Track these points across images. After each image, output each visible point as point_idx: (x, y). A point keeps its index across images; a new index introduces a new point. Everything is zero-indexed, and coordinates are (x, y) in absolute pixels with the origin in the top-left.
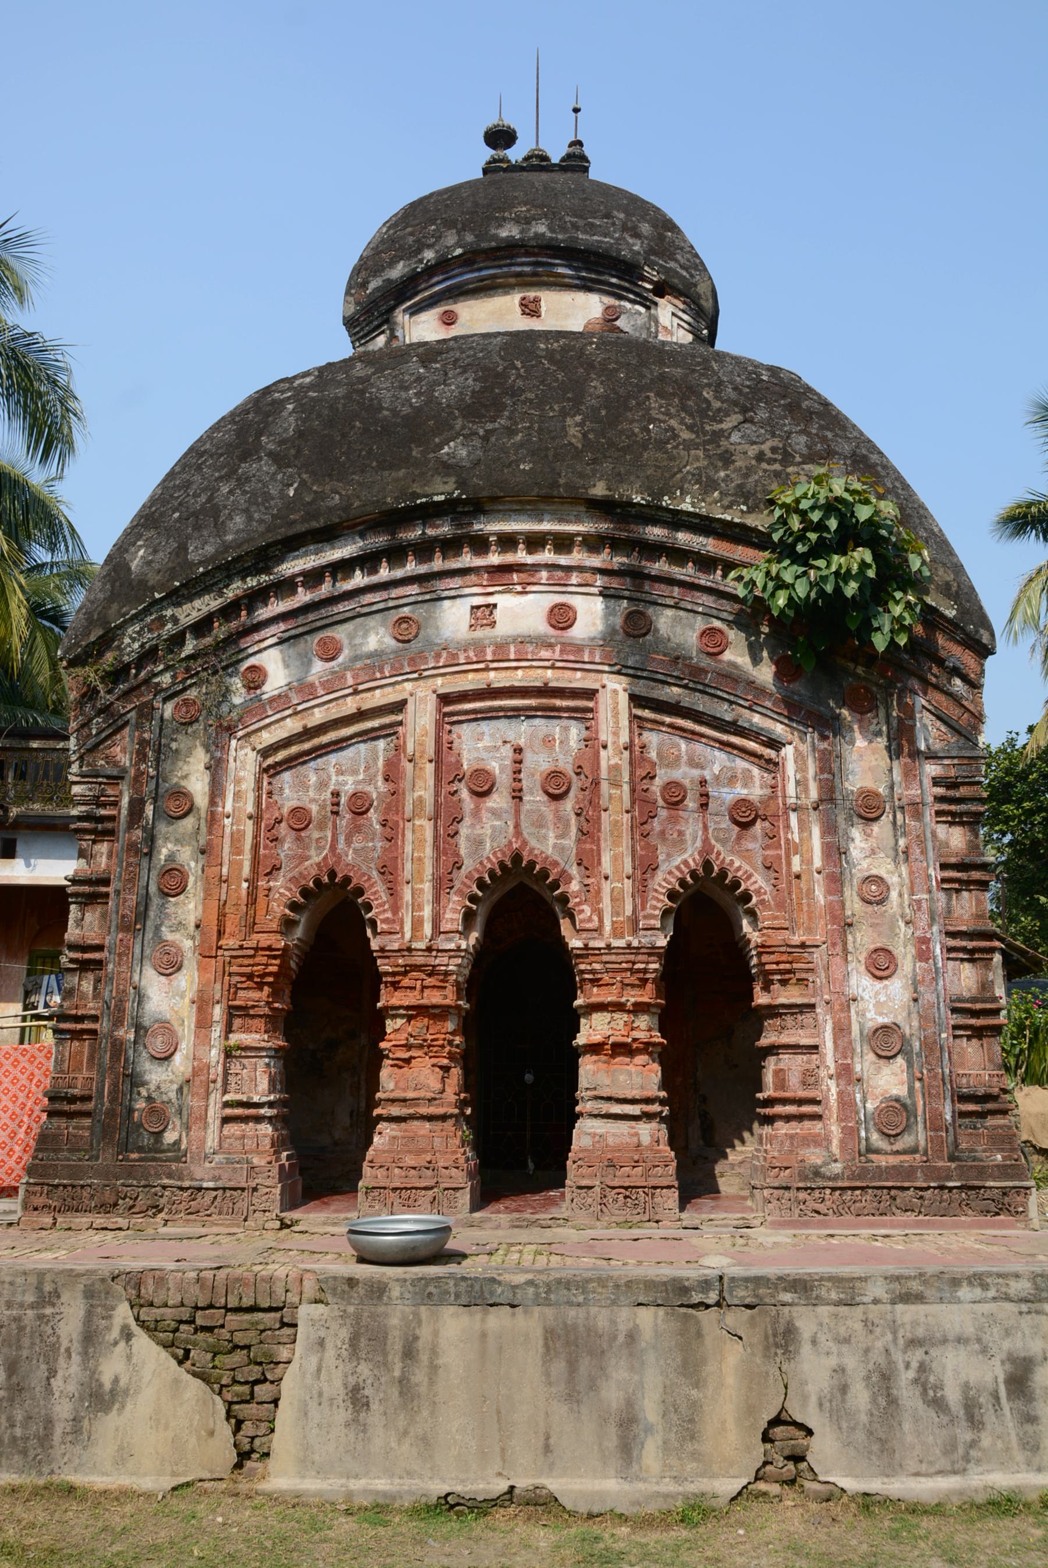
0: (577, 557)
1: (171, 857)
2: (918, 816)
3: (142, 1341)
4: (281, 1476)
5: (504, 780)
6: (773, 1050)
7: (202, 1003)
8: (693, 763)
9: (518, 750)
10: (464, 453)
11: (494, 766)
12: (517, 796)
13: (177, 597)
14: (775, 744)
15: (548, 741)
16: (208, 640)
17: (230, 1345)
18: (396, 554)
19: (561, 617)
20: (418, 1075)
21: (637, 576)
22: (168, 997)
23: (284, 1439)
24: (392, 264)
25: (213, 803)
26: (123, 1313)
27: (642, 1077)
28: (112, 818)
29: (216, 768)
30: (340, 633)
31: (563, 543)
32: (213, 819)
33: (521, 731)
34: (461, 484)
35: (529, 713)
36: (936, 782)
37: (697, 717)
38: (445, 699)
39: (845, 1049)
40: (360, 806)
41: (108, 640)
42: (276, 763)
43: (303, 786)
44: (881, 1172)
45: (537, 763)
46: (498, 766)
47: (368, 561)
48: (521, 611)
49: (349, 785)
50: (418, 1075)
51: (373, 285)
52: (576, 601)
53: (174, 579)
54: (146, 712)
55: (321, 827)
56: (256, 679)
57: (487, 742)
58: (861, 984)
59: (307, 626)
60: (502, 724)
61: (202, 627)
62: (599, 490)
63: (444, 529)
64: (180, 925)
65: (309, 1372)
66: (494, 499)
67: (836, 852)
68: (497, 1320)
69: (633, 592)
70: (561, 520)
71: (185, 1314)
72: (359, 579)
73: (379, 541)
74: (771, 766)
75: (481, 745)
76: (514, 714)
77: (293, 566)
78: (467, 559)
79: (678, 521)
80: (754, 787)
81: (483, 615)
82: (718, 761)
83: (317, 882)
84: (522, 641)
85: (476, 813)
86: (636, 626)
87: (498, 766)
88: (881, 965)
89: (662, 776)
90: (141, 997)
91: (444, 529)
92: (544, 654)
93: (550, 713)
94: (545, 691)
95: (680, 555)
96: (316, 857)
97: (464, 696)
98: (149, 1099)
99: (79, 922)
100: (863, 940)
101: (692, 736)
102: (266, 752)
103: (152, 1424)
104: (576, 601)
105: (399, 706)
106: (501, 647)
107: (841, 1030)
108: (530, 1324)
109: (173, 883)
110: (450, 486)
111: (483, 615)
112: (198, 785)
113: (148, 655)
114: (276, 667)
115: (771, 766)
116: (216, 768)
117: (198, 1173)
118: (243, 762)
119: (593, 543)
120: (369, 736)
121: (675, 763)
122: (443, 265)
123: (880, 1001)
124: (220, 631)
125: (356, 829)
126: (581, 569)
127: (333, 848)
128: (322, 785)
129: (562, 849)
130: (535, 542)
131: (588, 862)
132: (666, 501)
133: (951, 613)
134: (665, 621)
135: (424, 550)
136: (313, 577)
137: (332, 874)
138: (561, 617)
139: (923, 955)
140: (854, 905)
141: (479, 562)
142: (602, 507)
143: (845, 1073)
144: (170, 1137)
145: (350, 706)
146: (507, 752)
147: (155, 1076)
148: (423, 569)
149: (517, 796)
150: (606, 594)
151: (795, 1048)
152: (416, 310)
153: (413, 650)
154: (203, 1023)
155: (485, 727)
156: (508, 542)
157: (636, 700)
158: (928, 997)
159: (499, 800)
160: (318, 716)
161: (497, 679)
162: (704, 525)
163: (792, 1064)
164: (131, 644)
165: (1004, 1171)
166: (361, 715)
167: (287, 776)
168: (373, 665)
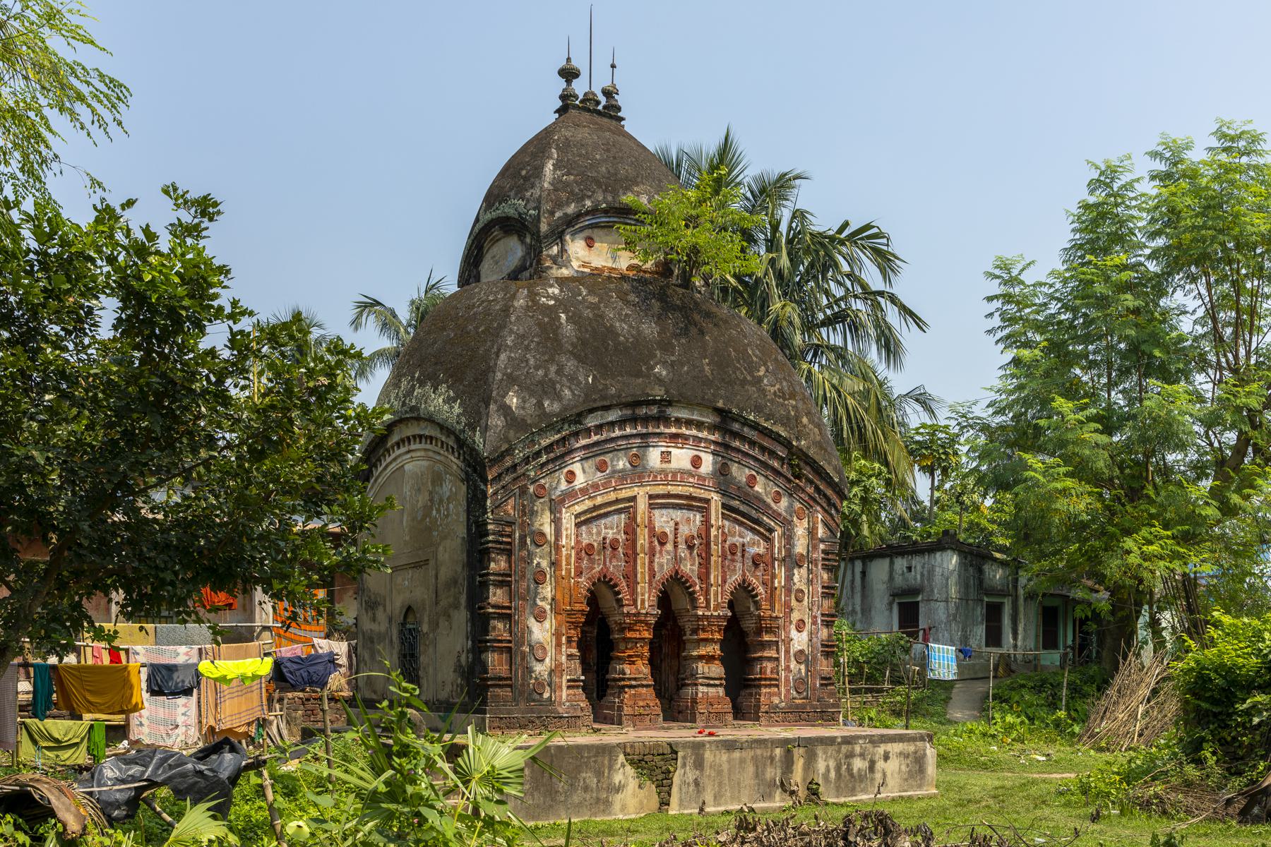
0: (704, 434)
1: (539, 563)
2: (816, 565)
3: (628, 768)
4: (673, 810)
5: (671, 537)
6: (761, 659)
7: (558, 635)
8: (741, 536)
9: (677, 524)
10: (664, 373)
11: (667, 530)
12: (676, 547)
13: (542, 431)
14: (771, 530)
15: (688, 520)
16: (552, 455)
17: (656, 767)
18: (634, 420)
19: (696, 462)
20: (636, 669)
21: (727, 446)
22: (541, 632)
23: (674, 800)
24: (568, 204)
25: (557, 539)
26: (621, 758)
27: (717, 670)
28: (509, 543)
29: (557, 522)
30: (607, 458)
31: (699, 425)
32: (558, 548)
33: (678, 515)
34: (667, 392)
35: (679, 507)
36: (823, 551)
37: (743, 515)
38: (651, 497)
39: (788, 659)
40: (614, 545)
41: (509, 451)
42: (583, 521)
43: (590, 533)
44: (797, 706)
45: (684, 530)
46: (669, 530)
47: (622, 423)
48: (681, 457)
49: (610, 534)
50: (635, 669)
51: (558, 215)
52: (702, 455)
53: (541, 421)
54: (523, 491)
55: (599, 554)
56: (571, 476)
57: (664, 519)
58: (794, 633)
59: (594, 451)
60: (671, 511)
61: (549, 449)
62: (720, 404)
63: (654, 410)
64: (544, 599)
65: (682, 776)
66: (678, 401)
67: (789, 578)
68: (737, 754)
69: (723, 451)
70: (701, 415)
71: (641, 757)
72: (617, 433)
73: (628, 412)
74: (768, 540)
75: (663, 520)
76: (675, 506)
77: (591, 422)
78: (662, 429)
79: (746, 423)
80: (760, 549)
81: (666, 457)
82: (749, 537)
83: (599, 580)
84: (683, 472)
85: (661, 552)
86: (722, 472)
87: (669, 530)
88: (800, 626)
89: (730, 540)
90: (530, 632)
91: (654, 410)
92: (691, 480)
93: (690, 508)
94: (690, 498)
95: (743, 438)
96: (597, 569)
97: (658, 496)
98: (536, 679)
99: (495, 594)
100: (795, 616)
101: (741, 524)
102: (577, 516)
103: (631, 796)
104: (702, 455)
105: (633, 499)
106: (674, 474)
107: (787, 652)
108: (748, 754)
109: (539, 578)
110: (662, 392)
111: (666, 457)
112: (548, 529)
113: (527, 460)
114: (582, 472)
115: (768, 540)
116: (557, 522)
117: (560, 710)
118: (568, 520)
119: (713, 428)
120: (619, 511)
121: (733, 535)
122: (593, 211)
123: (800, 640)
124: (558, 451)
125: (614, 556)
126: (706, 440)
127: (605, 563)
128: (599, 533)
129: (692, 571)
130: (689, 423)
131: (704, 577)
132: (744, 414)
133: (837, 480)
134: (734, 468)
135: (646, 420)
136: (599, 428)
137: (605, 577)
138: (696, 462)
139: (814, 623)
140: (794, 603)
141: (667, 431)
142: (719, 411)
143: (788, 668)
144: (546, 695)
145: (612, 496)
146: (672, 524)
147: (538, 668)
148: (644, 431)
149: (676, 547)
150: (714, 453)
151: (770, 659)
152: (573, 234)
153: (638, 472)
154: (559, 645)
155: (664, 511)
156: (678, 422)
157: (724, 506)
158: (815, 640)
159: (669, 547)
160: (599, 500)
161: (672, 489)
162: (755, 426)
163: (769, 666)
164: (519, 454)
165: (833, 706)
166: (617, 501)
167: (584, 528)
168: (623, 477)
